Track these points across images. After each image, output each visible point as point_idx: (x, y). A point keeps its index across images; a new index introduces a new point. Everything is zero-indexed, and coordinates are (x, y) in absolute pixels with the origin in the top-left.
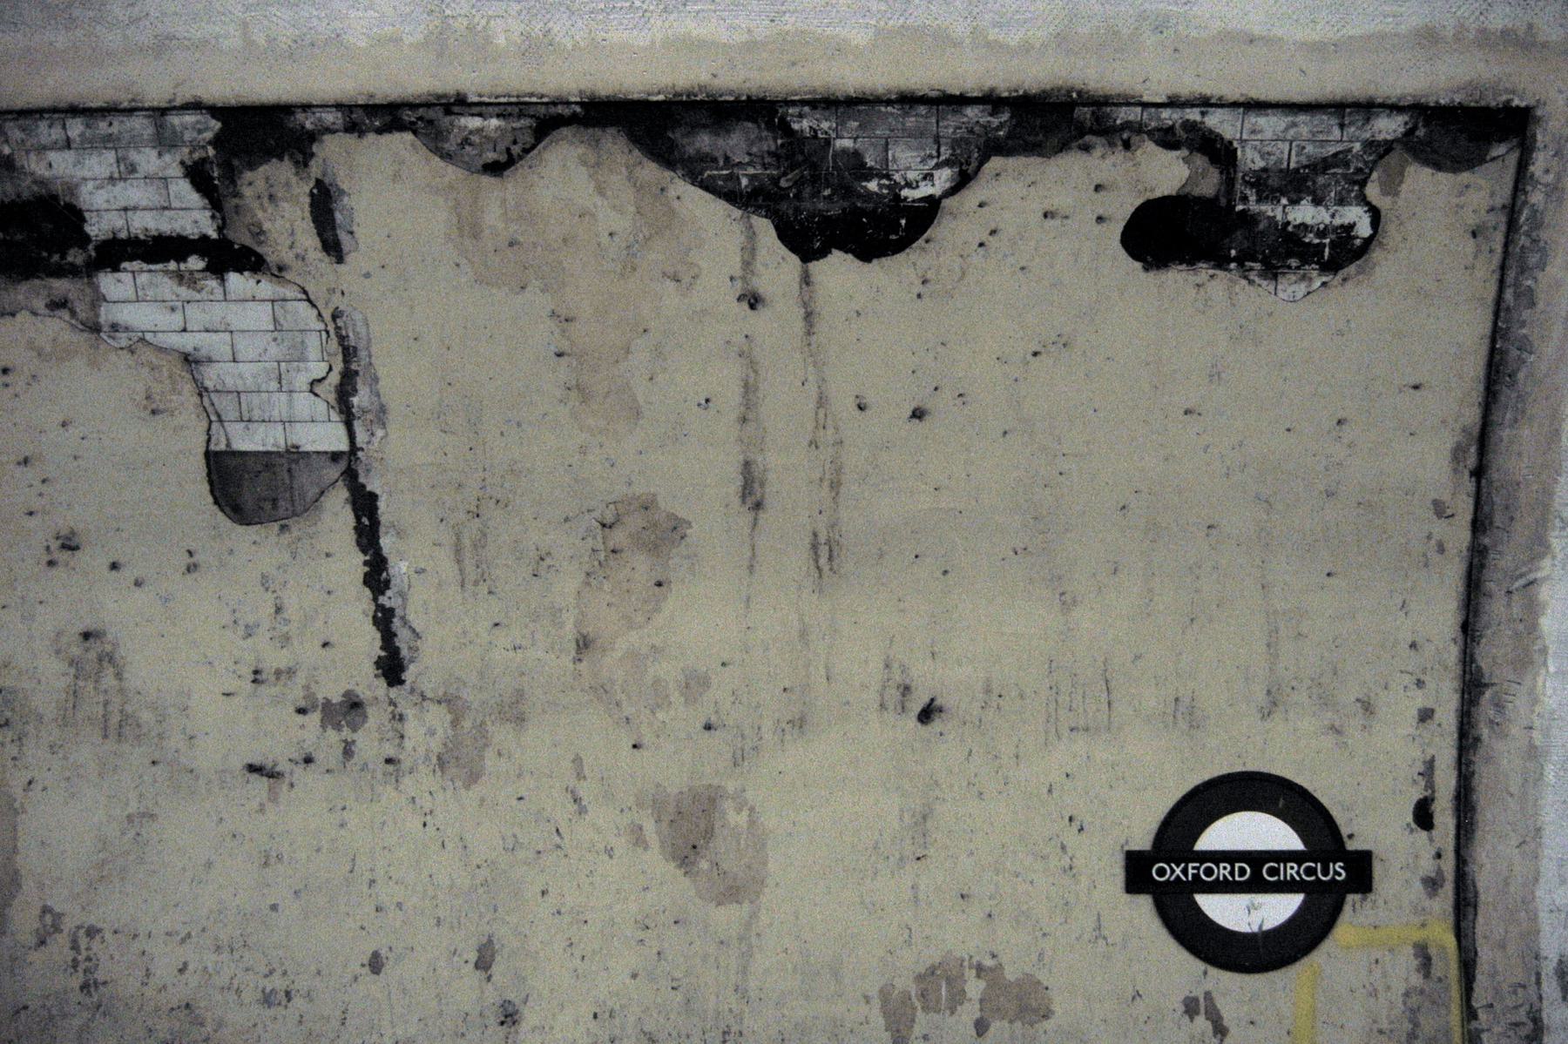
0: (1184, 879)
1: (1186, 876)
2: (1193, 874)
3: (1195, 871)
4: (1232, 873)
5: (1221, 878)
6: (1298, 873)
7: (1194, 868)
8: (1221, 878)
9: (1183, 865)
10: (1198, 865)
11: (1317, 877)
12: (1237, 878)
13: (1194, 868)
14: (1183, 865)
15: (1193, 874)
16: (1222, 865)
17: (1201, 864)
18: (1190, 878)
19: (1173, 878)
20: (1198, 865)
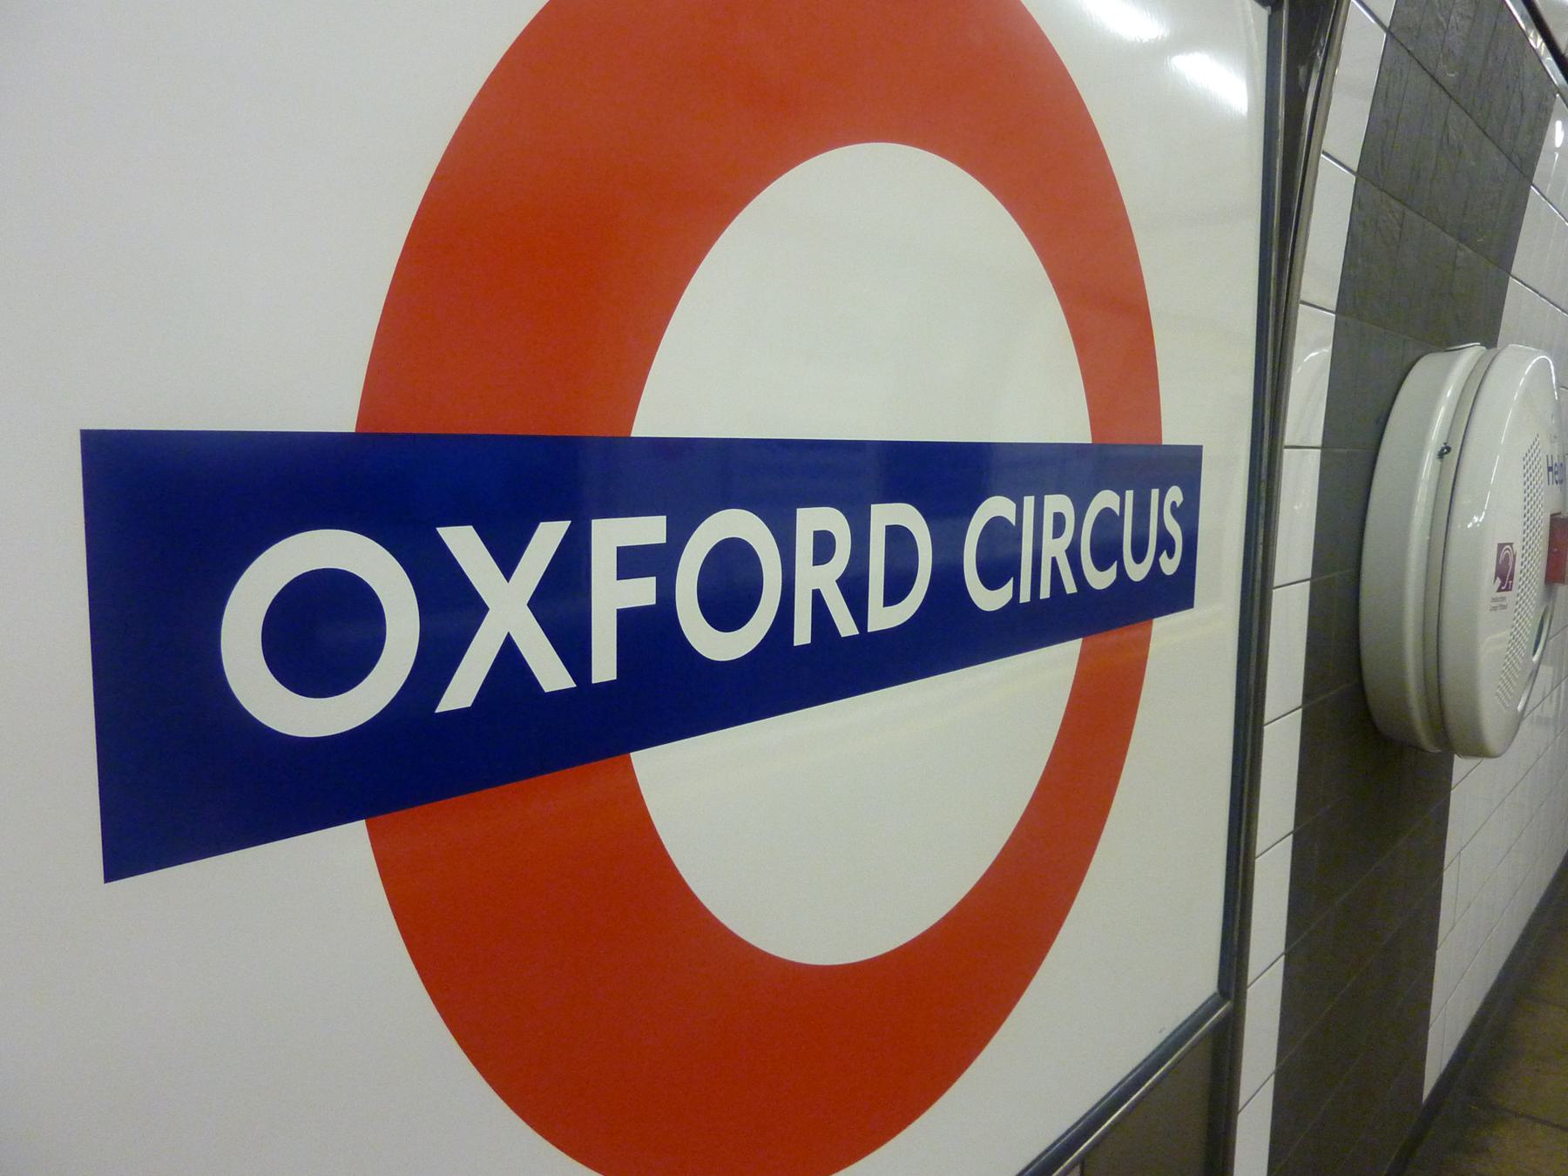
0: (552, 675)
1: (574, 650)
2: (628, 620)
3: (643, 592)
4: (854, 587)
5: (802, 634)
6: (1073, 553)
7: (631, 562)
8: (802, 634)
9: (548, 537)
10: (650, 530)
11: (1121, 571)
12: (883, 617)
13: (631, 562)
14: (548, 537)
15: (628, 620)
16: (811, 520)
17: (679, 535)
18: (604, 668)
19: (461, 692)
20: (650, 530)
